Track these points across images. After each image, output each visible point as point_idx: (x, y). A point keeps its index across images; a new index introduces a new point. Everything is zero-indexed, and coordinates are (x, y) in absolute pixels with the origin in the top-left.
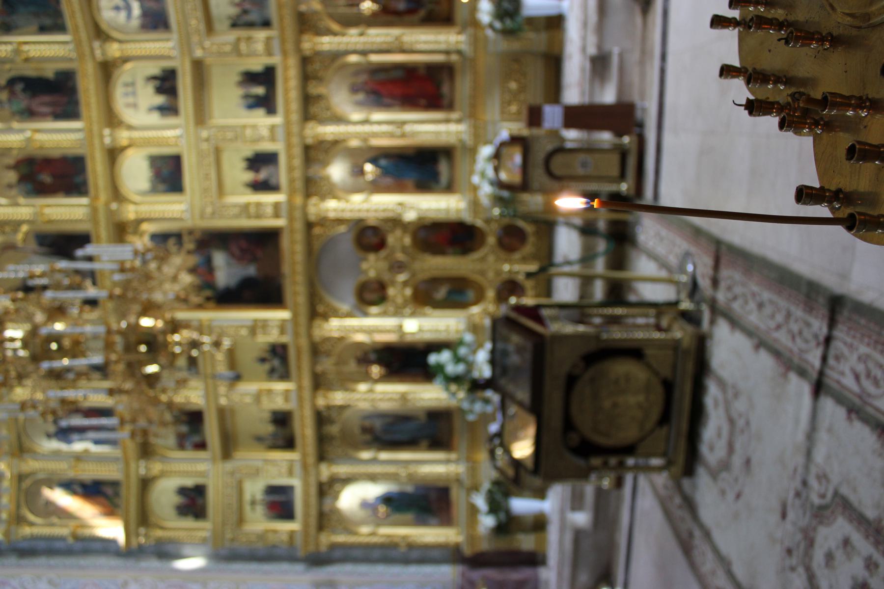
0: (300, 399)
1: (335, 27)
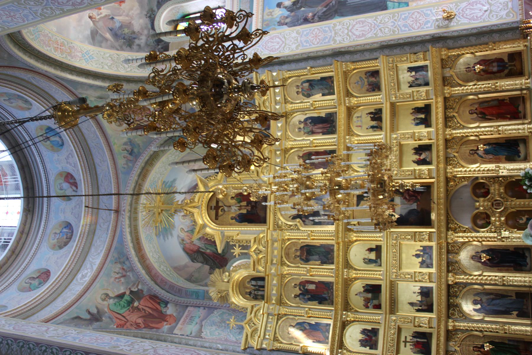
0: (440, 277)
1: (461, 82)
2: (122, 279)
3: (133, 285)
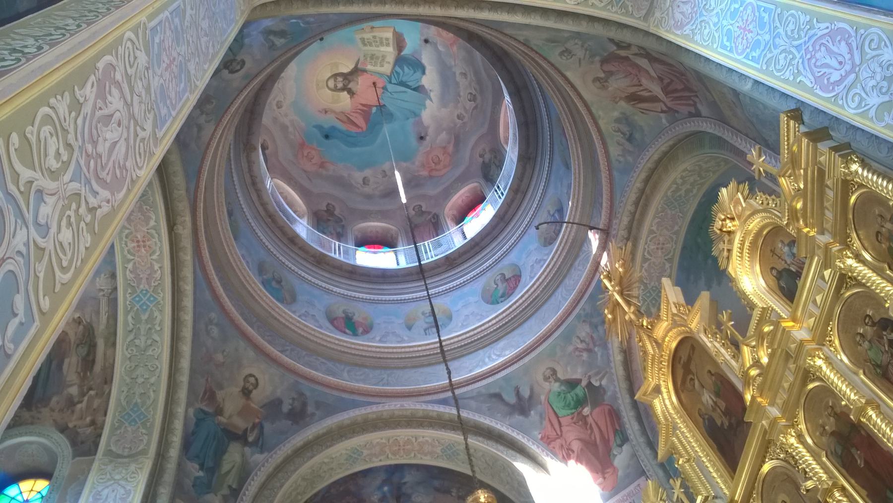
2: (585, 355)
3: (597, 374)
